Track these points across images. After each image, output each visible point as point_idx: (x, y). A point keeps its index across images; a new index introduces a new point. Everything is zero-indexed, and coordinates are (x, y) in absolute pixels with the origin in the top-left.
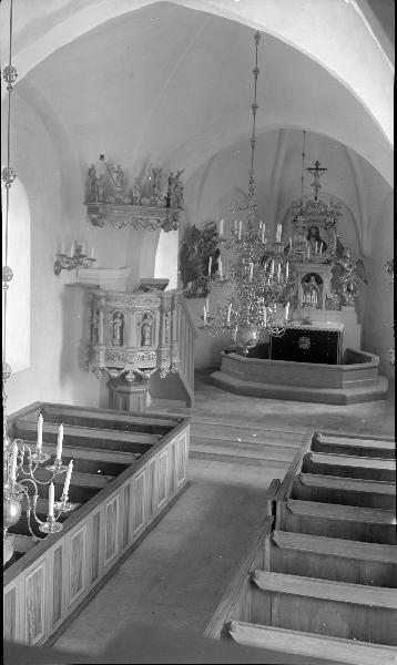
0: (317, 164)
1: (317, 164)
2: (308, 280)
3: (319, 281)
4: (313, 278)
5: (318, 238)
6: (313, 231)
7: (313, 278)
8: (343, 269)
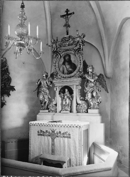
0: (67, 11)
1: (67, 11)
3: (71, 92)
4: (66, 90)
6: (67, 58)
7: (66, 90)
8: (88, 81)
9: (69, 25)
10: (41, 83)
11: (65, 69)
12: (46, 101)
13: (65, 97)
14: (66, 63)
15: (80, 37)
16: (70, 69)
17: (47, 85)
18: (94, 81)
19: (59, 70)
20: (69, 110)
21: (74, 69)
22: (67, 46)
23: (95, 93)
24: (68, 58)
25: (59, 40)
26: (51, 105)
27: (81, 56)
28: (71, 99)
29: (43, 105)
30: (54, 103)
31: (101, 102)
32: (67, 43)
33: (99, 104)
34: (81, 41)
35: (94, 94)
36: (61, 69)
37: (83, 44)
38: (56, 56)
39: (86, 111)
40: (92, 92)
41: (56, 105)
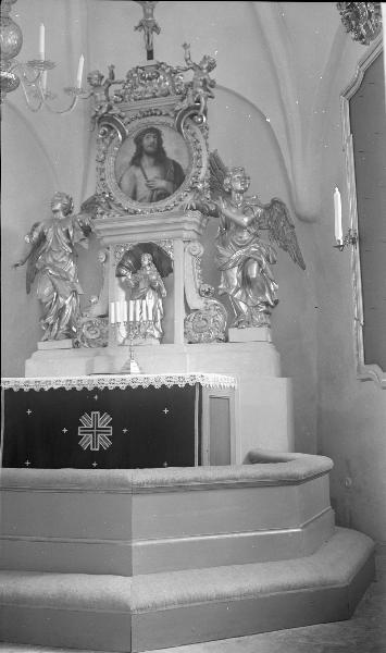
2: (137, 266)
3: (164, 266)
4: (146, 259)
5: (159, 156)
6: (148, 141)
7: (146, 259)
9: (156, 26)
10: (43, 238)
11: (142, 182)
12: (64, 306)
13: (142, 285)
14: (146, 161)
15: (196, 68)
16: (162, 184)
17: (70, 245)
18: (251, 223)
19: (119, 185)
20: (157, 334)
21: (174, 182)
22: (148, 98)
23: (255, 266)
24: (152, 140)
25: (121, 75)
26: (85, 320)
27: (200, 136)
28: (164, 291)
29: (50, 319)
30: (97, 310)
31: (276, 302)
32: (150, 89)
33: (270, 309)
34: (201, 83)
35: (254, 271)
36: (126, 183)
37: (208, 90)
38: (105, 133)
39: (222, 336)
40: (244, 264)
41: (105, 316)
